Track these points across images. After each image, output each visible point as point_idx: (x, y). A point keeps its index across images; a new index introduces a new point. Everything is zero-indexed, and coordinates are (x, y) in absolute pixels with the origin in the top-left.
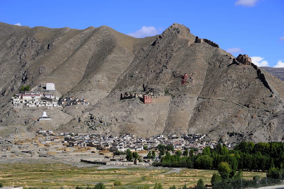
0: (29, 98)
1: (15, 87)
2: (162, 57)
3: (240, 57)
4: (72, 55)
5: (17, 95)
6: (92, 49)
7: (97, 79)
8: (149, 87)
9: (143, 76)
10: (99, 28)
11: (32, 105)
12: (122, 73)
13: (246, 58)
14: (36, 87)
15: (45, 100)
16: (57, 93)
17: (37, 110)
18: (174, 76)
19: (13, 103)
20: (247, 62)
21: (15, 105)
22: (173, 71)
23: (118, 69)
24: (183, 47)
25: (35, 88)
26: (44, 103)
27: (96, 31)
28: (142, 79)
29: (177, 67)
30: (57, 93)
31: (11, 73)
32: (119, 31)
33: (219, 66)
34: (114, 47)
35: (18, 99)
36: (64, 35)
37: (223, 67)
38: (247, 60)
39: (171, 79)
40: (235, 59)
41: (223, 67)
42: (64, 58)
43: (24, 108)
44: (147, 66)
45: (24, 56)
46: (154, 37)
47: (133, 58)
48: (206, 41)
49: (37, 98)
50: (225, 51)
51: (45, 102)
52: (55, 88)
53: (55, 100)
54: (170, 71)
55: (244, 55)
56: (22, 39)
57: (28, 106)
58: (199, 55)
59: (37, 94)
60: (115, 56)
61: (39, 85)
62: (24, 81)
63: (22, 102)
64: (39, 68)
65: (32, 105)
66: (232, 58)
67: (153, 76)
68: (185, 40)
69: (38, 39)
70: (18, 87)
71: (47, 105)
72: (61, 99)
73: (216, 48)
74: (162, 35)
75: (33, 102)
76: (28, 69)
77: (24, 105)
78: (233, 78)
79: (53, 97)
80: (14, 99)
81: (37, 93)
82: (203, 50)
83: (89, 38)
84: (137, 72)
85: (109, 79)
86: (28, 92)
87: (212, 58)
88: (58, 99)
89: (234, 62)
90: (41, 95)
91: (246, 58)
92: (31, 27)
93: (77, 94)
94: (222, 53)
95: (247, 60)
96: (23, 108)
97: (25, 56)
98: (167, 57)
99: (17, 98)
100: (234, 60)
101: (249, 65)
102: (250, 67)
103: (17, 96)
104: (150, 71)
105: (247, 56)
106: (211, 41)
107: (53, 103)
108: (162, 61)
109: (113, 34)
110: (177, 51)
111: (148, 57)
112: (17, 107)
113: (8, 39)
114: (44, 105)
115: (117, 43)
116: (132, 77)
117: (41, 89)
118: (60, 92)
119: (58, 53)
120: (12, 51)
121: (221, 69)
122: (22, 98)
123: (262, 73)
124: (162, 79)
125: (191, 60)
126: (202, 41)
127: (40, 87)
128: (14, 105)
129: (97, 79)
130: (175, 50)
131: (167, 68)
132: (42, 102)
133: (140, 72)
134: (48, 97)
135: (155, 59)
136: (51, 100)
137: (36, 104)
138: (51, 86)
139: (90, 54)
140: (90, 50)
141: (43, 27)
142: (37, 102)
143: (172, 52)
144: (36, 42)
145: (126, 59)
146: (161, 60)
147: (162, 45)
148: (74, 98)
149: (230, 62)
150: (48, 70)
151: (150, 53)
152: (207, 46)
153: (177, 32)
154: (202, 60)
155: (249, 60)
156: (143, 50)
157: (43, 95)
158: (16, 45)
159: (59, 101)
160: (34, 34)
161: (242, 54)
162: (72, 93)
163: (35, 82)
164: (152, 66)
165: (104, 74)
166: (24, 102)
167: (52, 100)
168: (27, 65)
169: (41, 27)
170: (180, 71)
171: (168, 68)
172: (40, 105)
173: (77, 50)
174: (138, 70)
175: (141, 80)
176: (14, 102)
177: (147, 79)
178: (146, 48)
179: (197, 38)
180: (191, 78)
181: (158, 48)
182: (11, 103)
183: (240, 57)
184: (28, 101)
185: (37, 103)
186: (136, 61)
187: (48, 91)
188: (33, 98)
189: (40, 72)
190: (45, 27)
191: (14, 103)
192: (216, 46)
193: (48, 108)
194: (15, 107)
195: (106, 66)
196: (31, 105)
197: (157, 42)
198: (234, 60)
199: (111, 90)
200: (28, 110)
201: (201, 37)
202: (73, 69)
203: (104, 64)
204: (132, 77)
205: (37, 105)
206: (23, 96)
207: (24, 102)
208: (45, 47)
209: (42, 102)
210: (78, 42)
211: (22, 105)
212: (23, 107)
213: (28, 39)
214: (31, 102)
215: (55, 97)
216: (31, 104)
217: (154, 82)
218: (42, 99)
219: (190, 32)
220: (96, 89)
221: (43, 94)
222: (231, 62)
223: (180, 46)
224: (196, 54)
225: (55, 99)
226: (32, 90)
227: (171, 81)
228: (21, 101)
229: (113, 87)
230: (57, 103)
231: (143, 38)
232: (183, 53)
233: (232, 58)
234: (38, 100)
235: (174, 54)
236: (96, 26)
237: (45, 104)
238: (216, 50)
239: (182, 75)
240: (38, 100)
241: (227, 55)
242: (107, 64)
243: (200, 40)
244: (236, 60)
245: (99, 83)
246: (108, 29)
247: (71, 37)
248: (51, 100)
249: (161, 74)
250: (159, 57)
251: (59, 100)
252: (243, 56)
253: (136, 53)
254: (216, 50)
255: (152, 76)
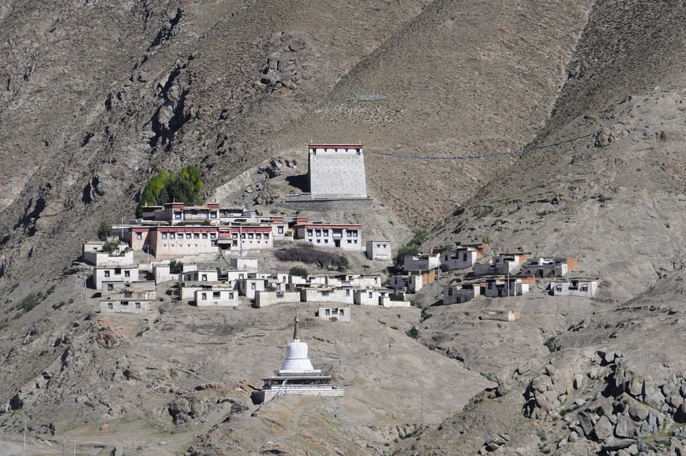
1: (105, 173)
5: (122, 227)
7: (656, 124)
14: (247, 178)
16: (383, 216)
17: (252, 331)
19: (91, 283)
25: (234, 182)
26: (297, 280)
30: (383, 220)
31: (78, 81)
35: (129, 256)
43: (164, 318)
51: (302, 273)
52: (370, 180)
57: (193, 303)
59: (249, 221)
61: (266, 164)
62: (164, 135)
63: (150, 276)
65: (217, 294)
70: (127, 174)
71: (313, 296)
75: (223, 278)
76: (191, 58)
77: (168, 298)
79: (351, 246)
80: (102, 259)
81: (252, 220)
86: (195, 212)
88: (385, 254)
90: (274, 227)
96: (156, 315)
99: (123, 247)
103: (117, 233)
107: (357, 282)
112: (117, 306)
114: (294, 297)
117: (278, 193)
118: (402, 209)
122: (150, 248)
127: (271, 173)
128: (98, 295)
134: (322, 242)
136: (338, 265)
137: (240, 287)
142: (251, 276)
148: (495, 249)
157: (286, 228)
159: (392, 271)
162: (479, 216)
163: (238, 145)
166: (164, 274)
167: (351, 262)
168: (189, 32)
172: (266, 299)
176: (100, 274)
182: (79, 280)
184: (193, 268)
185: (249, 283)
187: (323, 204)
188: (225, 247)
189: (273, 76)
191: (99, 285)
193: (323, 315)
194: (109, 311)
196: (210, 294)
200: (194, 328)
202: (491, 54)
205: (250, 294)
206: (159, 235)
207: (164, 274)
209: (280, 277)
211: (151, 292)
212: (161, 312)
214: (213, 277)
215: (369, 245)
218: (284, 255)
220: (644, 192)
221: (291, 225)
225: (368, 255)
226: (221, 195)
228: (143, 267)
230: (379, 285)
234: (253, 264)
237: (299, 288)
240: (253, 264)
245: (670, 147)
248: (338, 265)
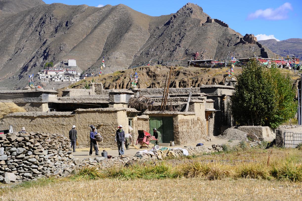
0: (54, 74)
2: (176, 35)
3: (246, 36)
4: (91, 33)
5: (43, 70)
6: (110, 27)
7: (116, 56)
8: (163, 64)
9: (159, 53)
10: (117, 6)
11: (57, 80)
12: (138, 51)
13: (252, 37)
14: (59, 63)
15: (68, 75)
16: (79, 69)
17: (62, 85)
18: (186, 54)
19: (39, 78)
20: (253, 41)
21: (41, 79)
22: (186, 49)
23: (135, 46)
24: (196, 26)
25: (57, 64)
26: (68, 78)
27: (113, 9)
28: (157, 57)
29: (190, 46)
30: (79, 69)
32: (135, 9)
33: (228, 45)
34: (130, 25)
35: (44, 74)
36: (82, 12)
37: (231, 45)
38: (253, 40)
39: (183, 57)
40: (242, 38)
41: (231, 45)
42: (83, 36)
43: (50, 83)
44: (162, 44)
45: (43, 32)
46: (168, 16)
47: (149, 36)
48: (216, 21)
49: (61, 74)
50: (234, 30)
51: (69, 77)
52: (77, 64)
53: (77, 75)
54: (183, 49)
55: (250, 35)
56: (40, 16)
57: (54, 81)
58: (210, 34)
59: (60, 69)
60: (132, 34)
61: (62, 61)
63: (47, 77)
64: (60, 45)
65: (57, 80)
66: (240, 37)
67: (168, 54)
68: (198, 20)
69: (56, 16)
71: (70, 80)
72: (82, 75)
73: (226, 28)
74: (176, 14)
75: (58, 77)
76: (49, 46)
77: (50, 80)
78: (239, 56)
79: (75, 73)
80: (40, 75)
81: (60, 69)
82: (214, 29)
83: (107, 16)
84: (153, 50)
85: (127, 56)
86: (52, 68)
87: (222, 37)
88: (79, 74)
89: (241, 41)
90: (64, 70)
91: (252, 37)
92: (47, 4)
93: (97, 70)
94: (231, 33)
95: (253, 40)
96: (49, 82)
97: (44, 32)
98: (180, 36)
99: (43, 73)
100: (241, 39)
101: (254, 43)
102: (256, 45)
103: (42, 71)
104: (165, 49)
105: (253, 35)
106: (221, 21)
107: (76, 78)
108: (176, 40)
109: (130, 13)
110: (190, 30)
111: (163, 35)
112: (43, 81)
113: (26, 15)
114: (68, 80)
115: (134, 22)
116: (148, 54)
117: (64, 65)
118: (81, 68)
119: (78, 31)
120: (31, 27)
121: (229, 48)
122: (46, 73)
123: (265, 51)
124: (175, 57)
125: (202, 39)
126: (213, 21)
127: (62, 63)
128: (40, 80)
129: (116, 56)
130: (188, 29)
131: (180, 47)
132: (65, 77)
133: (155, 50)
134: (70, 72)
135: (169, 38)
136: (73, 76)
137: (60, 78)
138: (72, 63)
139: (108, 32)
140: (108, 28)
141: (61, 4)
142: (62, 77)
143: (185, 31)
144: (55, 19)
145: (143, 38)
146: (174, 39)
147: (176, 23)
148: (95, 74)
149: (238, 41)
150: (68, 47)
151: (165, 32)
152: (217, 26)
153: (190, 12)
154: (213, 39)
155: (255, 39)
156: (159, 29)
157: (65, 71)
158: (35, 21)
159: (80, 77)
160: (53, 11)
161: (249, 34)
162: (92, 69)
163: (57, 59)
164: (166, 45)
165: (122, 51)
166: (49, 77)
167: (74, 75)
168: (48, 43)
169: (59, 4)
170: (192, 50)
171: (181, 47)
172: (64, 80)
173: (96, 27)
174: (153, 48)
175: (156, 58)
176: (40, 77)
177: (162, 57)
178: (162, 26)
179: (208, 18)
180: (202, 56)
181: (173, 27)
182: (37, 78)
183: (247, 37)
184: (53, 76)
185: (62, 78)
186: (152, 39)
187: (70, 67)
188: (57, 73)
189: (61, 49)
190: (63, 4)
191: (40, 78)
192: (226, 26)
193: (72, 82)
194: (42, 82)
195: (124, 43)
196: (56, 80)
197: (171, 21)
198: (241, 39)
199: (128, 67)
200: (54, 84)
201: (213, 18)
203: (121, 42)
204: (148, 54)
205: (62, 80)
206: (48, 71)
207: (49, 77)
208: (64, 24)
209: (65, 77)
210: (96, 20)
211: (48, 79)
212: (50, 82)
213: (47, 16)
214: (56, 77)
215: (77, 73)
216: (56, 79)
217: (168, 60)
218: (66, 74)
219: (203, 11)
220: (115, 66)
221: (66, 70)
222: (239, 41)
223: (192, 25)
224: (207, 34)
225: (77, 74)
226: (55, 66)
227: (184, 59)
228: (46, 76)
229: (131, 63)
230: (79, 78)
231: (158, 17)
232: (195, 33)
233: (240, 37)
234: (62, 75)
235: (187, 33)
236: (113, 4)
237: (68, 79)
238: (226, 30)
239: (194, 53)
240: (62, 75)
241: (235, 35)
242: (124, 41)
243: (211, 20)
244: (243, 39)
245: (118, 59)
246: (124, 7)
247: (89, 15)
248: (73, 76)
249: (175, 51)
250: (173, 36)
251: (80, 75)
252: (249, 36)
253: (151, 31)
254: (226, 30)
255: (167, 53)
